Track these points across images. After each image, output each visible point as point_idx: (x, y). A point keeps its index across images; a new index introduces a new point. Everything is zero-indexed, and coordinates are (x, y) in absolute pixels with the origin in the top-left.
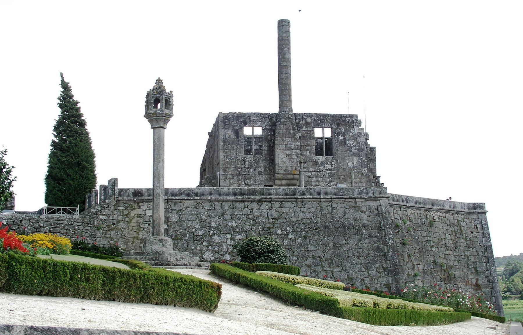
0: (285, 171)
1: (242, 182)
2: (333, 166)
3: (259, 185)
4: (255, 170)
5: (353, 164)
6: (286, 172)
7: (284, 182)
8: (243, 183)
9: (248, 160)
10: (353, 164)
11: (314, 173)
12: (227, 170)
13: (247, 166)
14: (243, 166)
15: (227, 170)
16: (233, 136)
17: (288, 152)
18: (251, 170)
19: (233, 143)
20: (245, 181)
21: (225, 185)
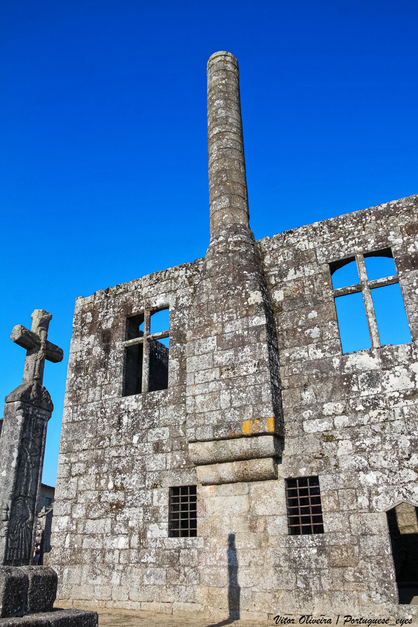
1: (107, 482)
8: (111, 485)
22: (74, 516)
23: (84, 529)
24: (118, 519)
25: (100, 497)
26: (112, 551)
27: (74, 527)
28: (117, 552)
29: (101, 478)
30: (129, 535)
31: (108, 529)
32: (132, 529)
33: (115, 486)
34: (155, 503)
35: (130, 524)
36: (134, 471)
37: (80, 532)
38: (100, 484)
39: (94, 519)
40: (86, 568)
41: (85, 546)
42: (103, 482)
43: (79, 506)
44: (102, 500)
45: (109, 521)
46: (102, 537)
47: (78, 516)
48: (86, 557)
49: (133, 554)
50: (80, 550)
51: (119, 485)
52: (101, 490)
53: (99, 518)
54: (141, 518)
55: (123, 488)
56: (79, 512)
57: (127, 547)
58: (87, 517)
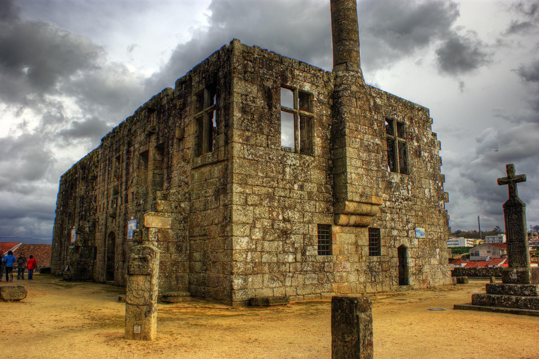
0: (361, 196)
1: (278, 214)
2: (410, 192)
3: (309, 222)
4: (301, 188)
5: (430, 191)
6: (364, 199)
7: (353, 219)
8: (281, 217)
9: (289, 162)
10: (430, 191)
11: (388, 204)
12: (250, 181)
13: (288, 177)
14: (280, 176)
15: (250, 181)
16: (260, 102)
17: (364, 155)
18: (296, 187)
19: (261, 117)
20: (283, 213)
21: (244, 219)
22: (254, 237)
23: (262, 248)
24: (287, 242)
25: (273, 225)
26: (284, 264)
27: (254, 246)
28: (288, 265)
29: (273, 211)
30: (295, 253)
31: (281, 249)
32: (296, 249)
33: (284, 218)
34: (311, 233)
35: (296, 245)
36: (296, 209)
37: (259, 249)
38: (272, 215)
39: (270, 241)
40: (267, 276)
41: (264, 260)
42: (275, 214)
43: (257, 230)
44: (275, 227)
45: (281, 243)
46: (277, 254)
47: (256, 238)
48: (266, 268)
49: (298, 265)
50: (261, 263)
51: (286, 217)
52: (274, 220)
53: (272, 240)
54: (302, 242)
55: (289, 221)
56: (258, 235)
57: (294, 261)
58: (264, 239)
